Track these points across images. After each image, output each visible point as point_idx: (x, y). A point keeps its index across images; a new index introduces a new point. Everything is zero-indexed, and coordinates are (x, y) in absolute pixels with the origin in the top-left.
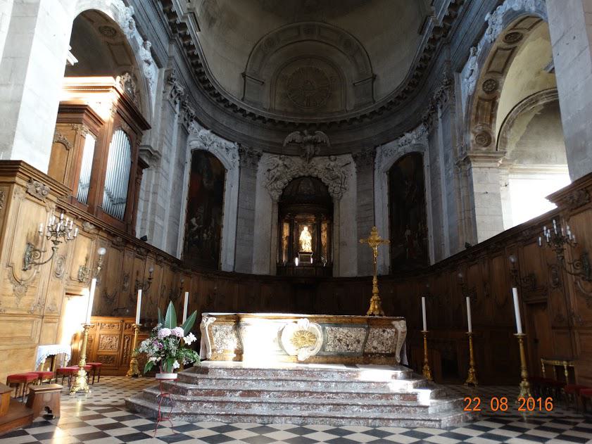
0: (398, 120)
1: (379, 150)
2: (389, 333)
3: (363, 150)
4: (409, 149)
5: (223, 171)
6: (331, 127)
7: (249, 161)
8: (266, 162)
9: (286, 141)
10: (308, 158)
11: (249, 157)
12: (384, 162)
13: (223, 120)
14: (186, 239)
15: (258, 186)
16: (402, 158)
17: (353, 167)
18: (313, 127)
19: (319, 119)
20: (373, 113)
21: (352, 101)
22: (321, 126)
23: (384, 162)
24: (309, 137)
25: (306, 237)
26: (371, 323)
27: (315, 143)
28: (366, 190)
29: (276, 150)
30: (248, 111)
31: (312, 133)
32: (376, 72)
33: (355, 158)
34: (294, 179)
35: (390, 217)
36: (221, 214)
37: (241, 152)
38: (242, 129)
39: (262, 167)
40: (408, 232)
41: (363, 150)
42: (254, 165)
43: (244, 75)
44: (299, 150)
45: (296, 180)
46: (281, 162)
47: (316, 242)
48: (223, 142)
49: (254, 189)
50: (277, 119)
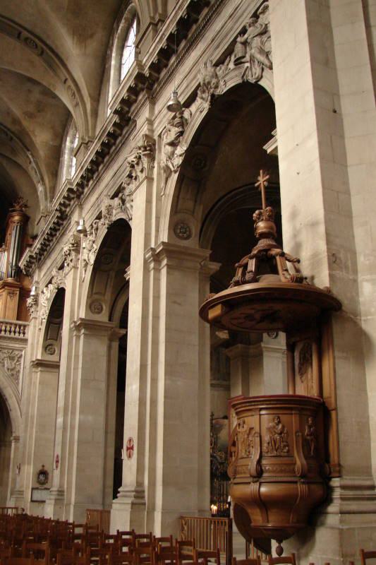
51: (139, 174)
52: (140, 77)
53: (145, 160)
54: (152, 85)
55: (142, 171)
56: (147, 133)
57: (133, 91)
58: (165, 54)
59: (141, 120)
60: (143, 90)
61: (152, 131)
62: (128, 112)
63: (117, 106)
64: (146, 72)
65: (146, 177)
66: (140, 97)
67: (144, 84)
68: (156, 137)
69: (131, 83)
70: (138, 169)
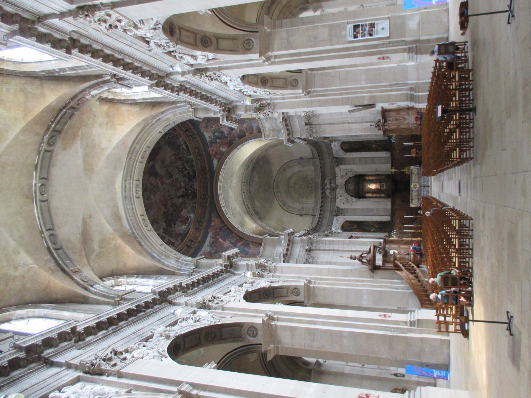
0: (325, 150)
1: (335, 156)
2: (414, 170)
3: (335, 162)
4: (339, 145)
5: (347, 222)
6: (323, 178)
7: (341, 211)
8: (340, 203)
9: (330, 196)
10: (337, 186)
11: (339, 212)
12: (342, 154)
13: (325, 222)
14: (380, 232)
15: (352, 207)
16: (342, 148)
17: (341, 166)
18: (323, 184)
19: (319, 180)
20: (320, 159)
21: (312, 168)
22: (323, 180)
23: (342, 154)
24: (328, 186)
25: (373, 186)
26: (412, 173)
27: (330, 183)
28: (353, 161)
29: (334, 199)
30: (319, 212)
31: (326, 185)
32: (299, 158)
33: (338, 166)
34: (346, 192)
35: (366, 151)
36: (366, 222)
37: (337, 215)
38: (327, 215)
39: (342, 206)
40: (374, 146)
41: (335, 162)
42: (342, 209)
43: (301, 215)
44: (333, 190)
45: (347, 191)
46: (339, 198)
47: (372, 182)
48: (334, 222)
49: (353, 209)
50: (321, 200)
51: (217, 75)
52: (157, 85)
53: (208, 74)
54: (159, 77)
55: (215, 74)
56: (191, 75)
57: (166, 87)
58: (135, 70)
59: (181, 78)
60: (164, 81)
61: (189, 72)
62: (177, 87)
63: (175, 94)
64: (154, 82)
65: (219, 71)
66: (169, 82)
67: (161, 81)
68: (193, 68)
69: (161, 89)
70: (213, 76)
